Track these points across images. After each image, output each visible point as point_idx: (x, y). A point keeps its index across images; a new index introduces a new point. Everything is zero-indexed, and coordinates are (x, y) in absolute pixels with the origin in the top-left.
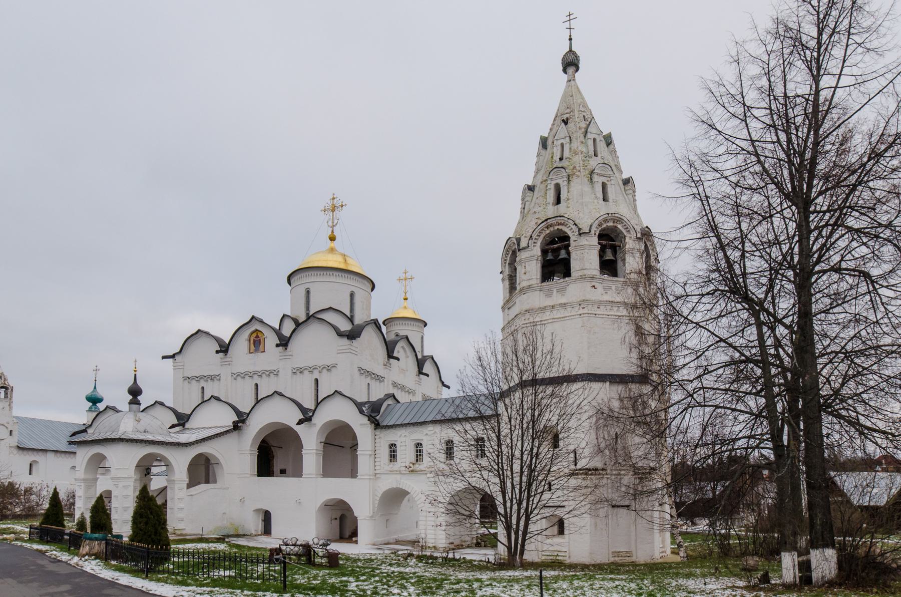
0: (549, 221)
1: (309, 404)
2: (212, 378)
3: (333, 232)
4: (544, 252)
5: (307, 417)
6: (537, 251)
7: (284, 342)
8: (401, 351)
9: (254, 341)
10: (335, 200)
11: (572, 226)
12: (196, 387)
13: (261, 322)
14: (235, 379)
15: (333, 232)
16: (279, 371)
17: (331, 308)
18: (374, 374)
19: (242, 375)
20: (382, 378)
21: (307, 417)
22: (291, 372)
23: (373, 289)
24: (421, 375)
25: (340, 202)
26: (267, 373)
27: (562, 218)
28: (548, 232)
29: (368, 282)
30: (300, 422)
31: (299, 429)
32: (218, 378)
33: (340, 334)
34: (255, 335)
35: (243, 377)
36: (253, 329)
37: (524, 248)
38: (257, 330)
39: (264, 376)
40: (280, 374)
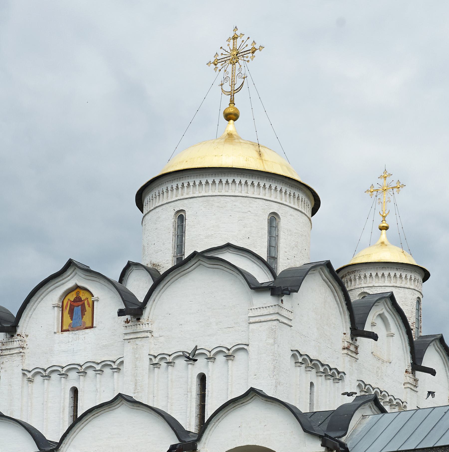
3: (232, 102)
8: (379, 322)
10: (239, 41)
13: (87, 271)
14: (30, 381)
15: (232, 102)
16: (122, 362)
18: (323, 365)
20: (339, 373)
22: (147, 362)
23: (314, 210)
24: (418, 373)
25: (249, 42)
26: (98, 367)
29: (304, 193)
34: (72, 297)
35: (48, 377)
36: (70, 284)
38: (77, 287)
39: (90, 372)
40: (124, 368)
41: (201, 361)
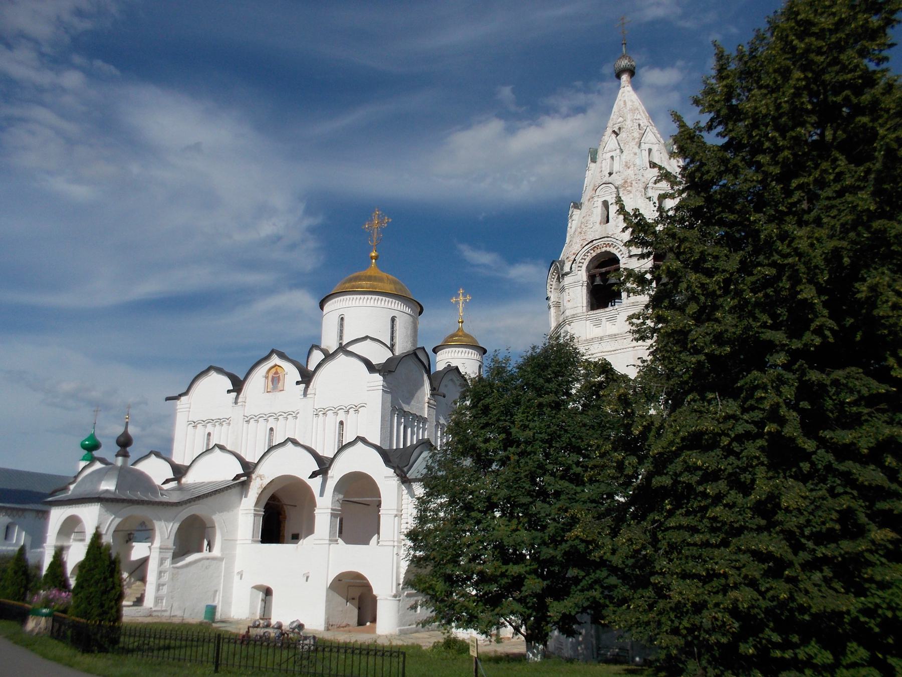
0: (594, 242)
1: (327, 452)
2: (220, 422)
4: (591, 277)
5: (324, 466)
6: (582, 275)
7: (306, 377)
9: (273, 378)
11: (621, 248)
12: (201, 431)
17: (366, 338)
19: (257, 418)
21: (324, 466)
26: (285, 415)
27: (609, 239)
28: (594, 254)
30: (314, 475)
31: (315, 484)
32: (228, 421)
33: (371, 367)
37: (567, 274)
41: (341, 412)
